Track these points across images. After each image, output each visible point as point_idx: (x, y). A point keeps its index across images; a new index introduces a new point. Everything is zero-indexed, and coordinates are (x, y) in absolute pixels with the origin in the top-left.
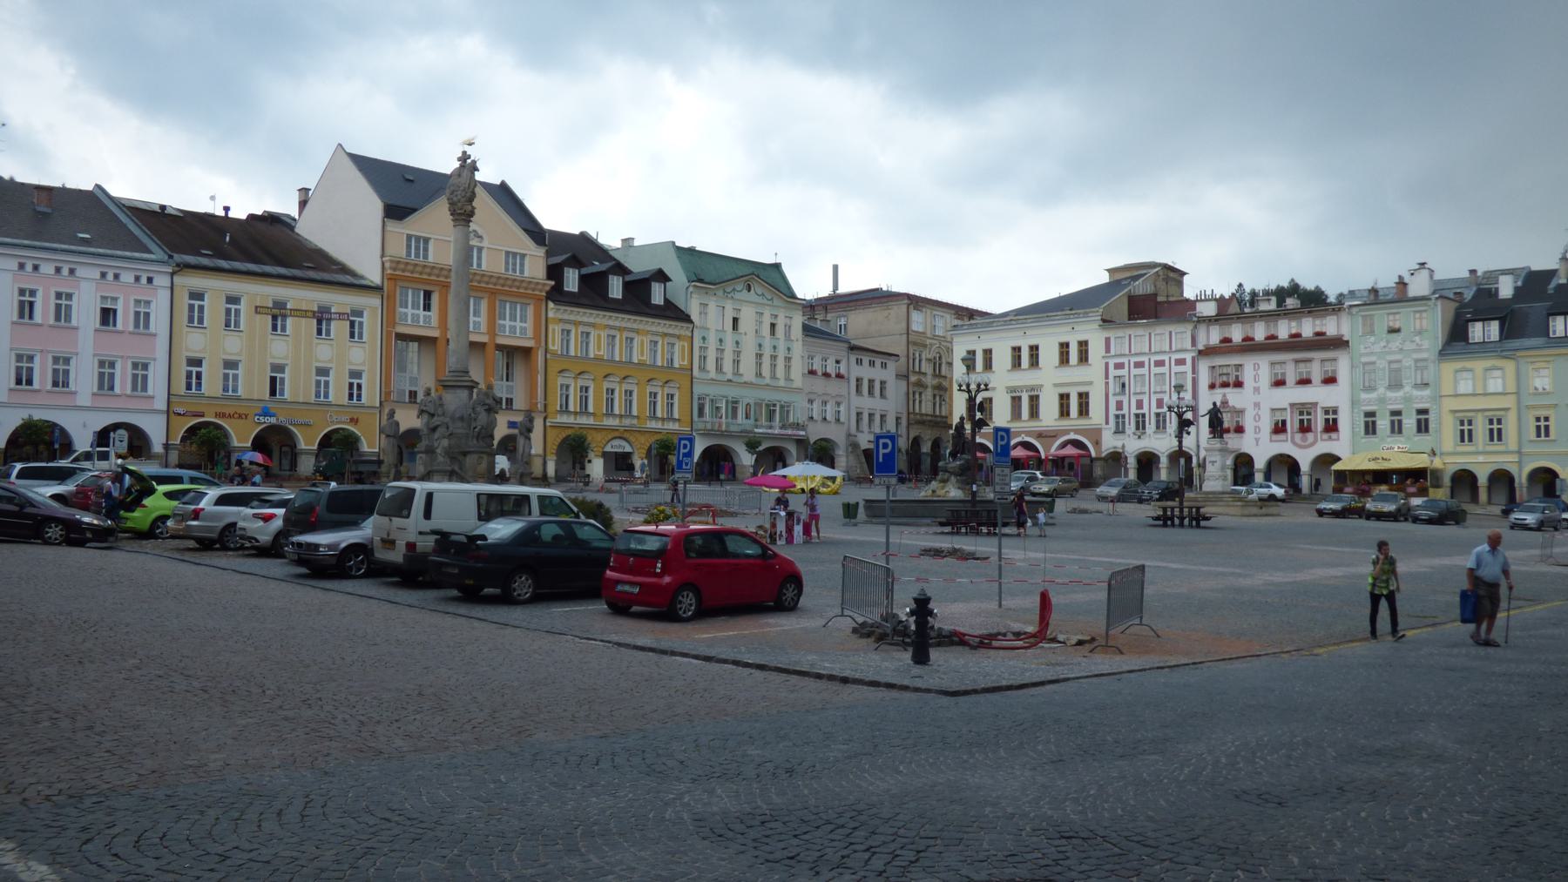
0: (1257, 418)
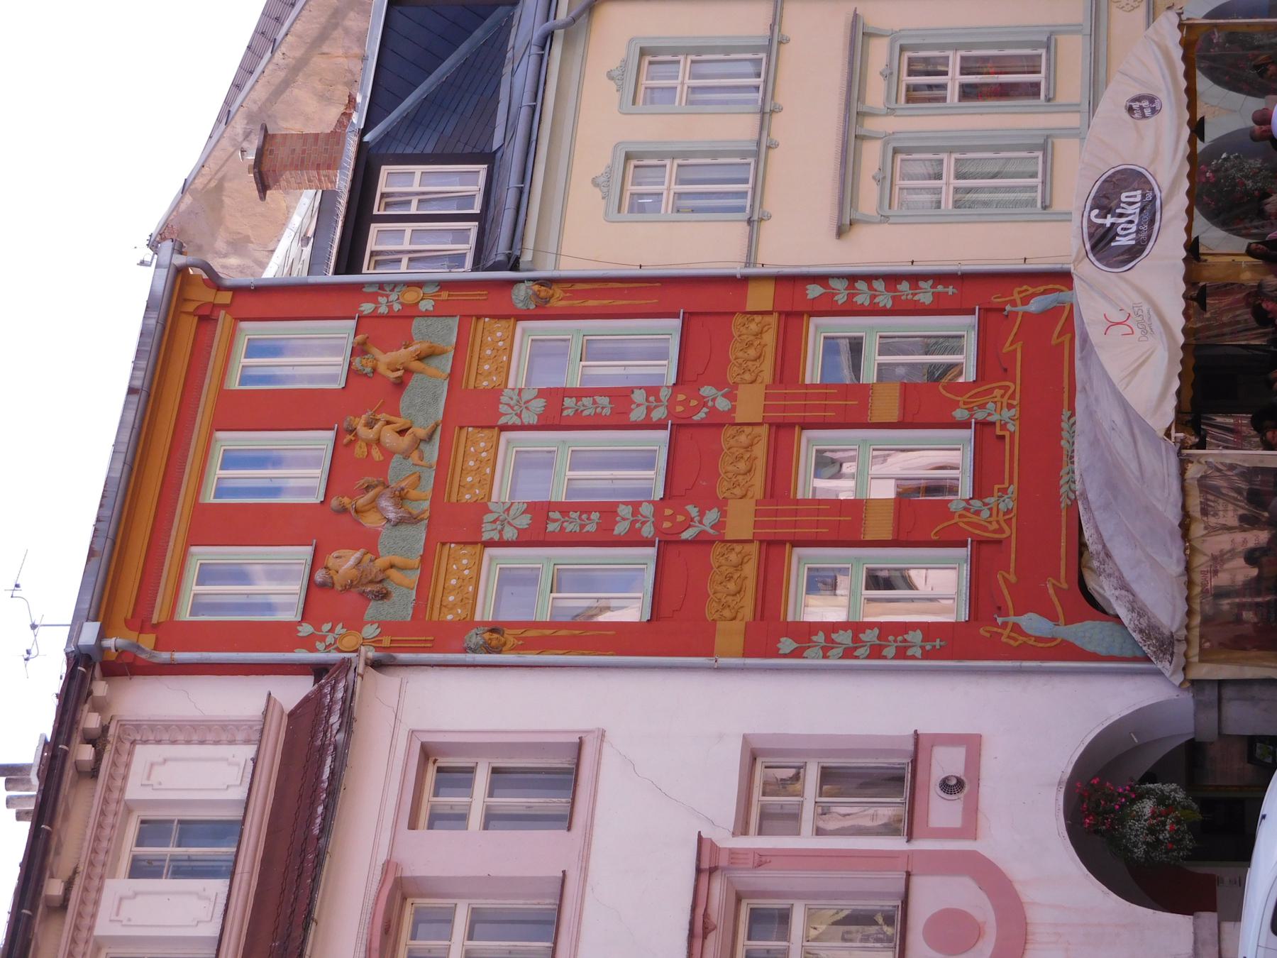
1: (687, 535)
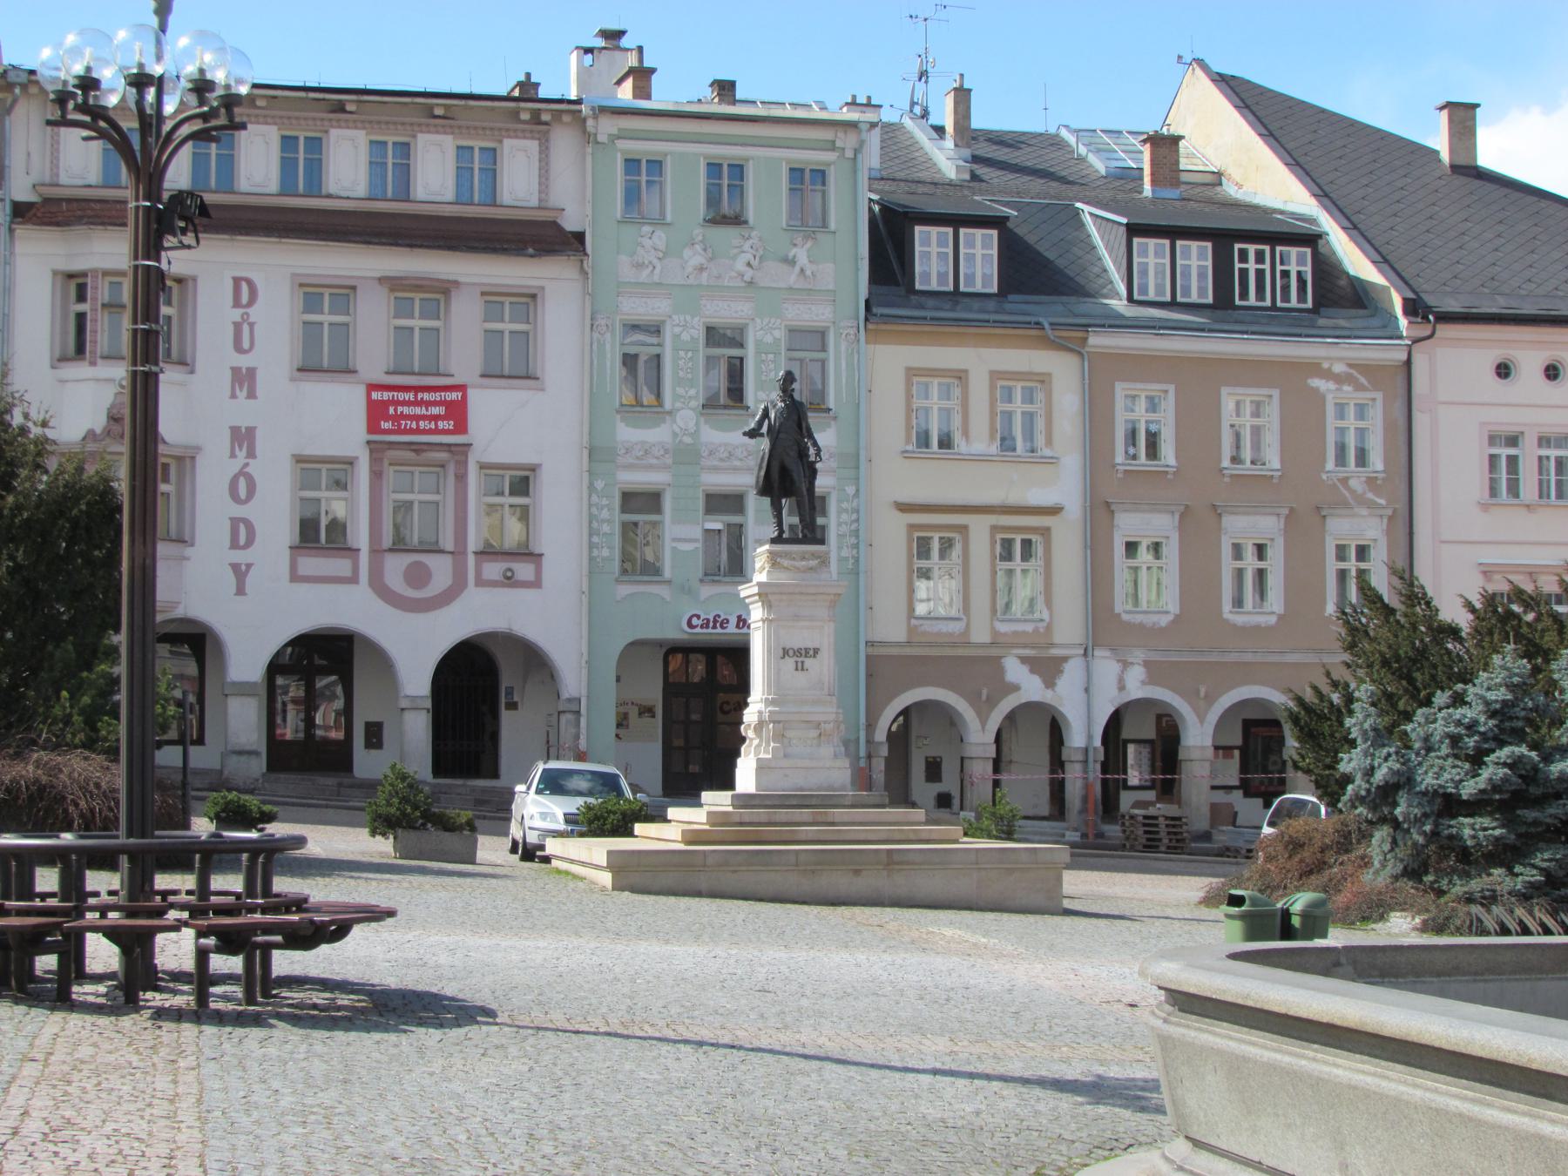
0: (242, 487)
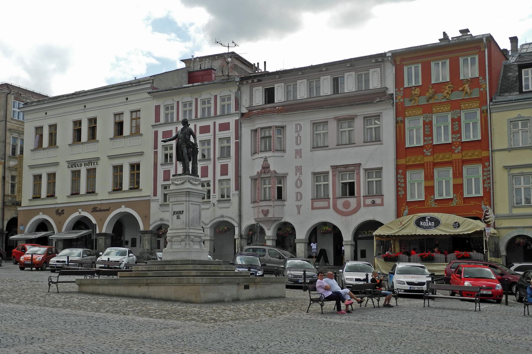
0: (299, 183)
1: (425, 150)
